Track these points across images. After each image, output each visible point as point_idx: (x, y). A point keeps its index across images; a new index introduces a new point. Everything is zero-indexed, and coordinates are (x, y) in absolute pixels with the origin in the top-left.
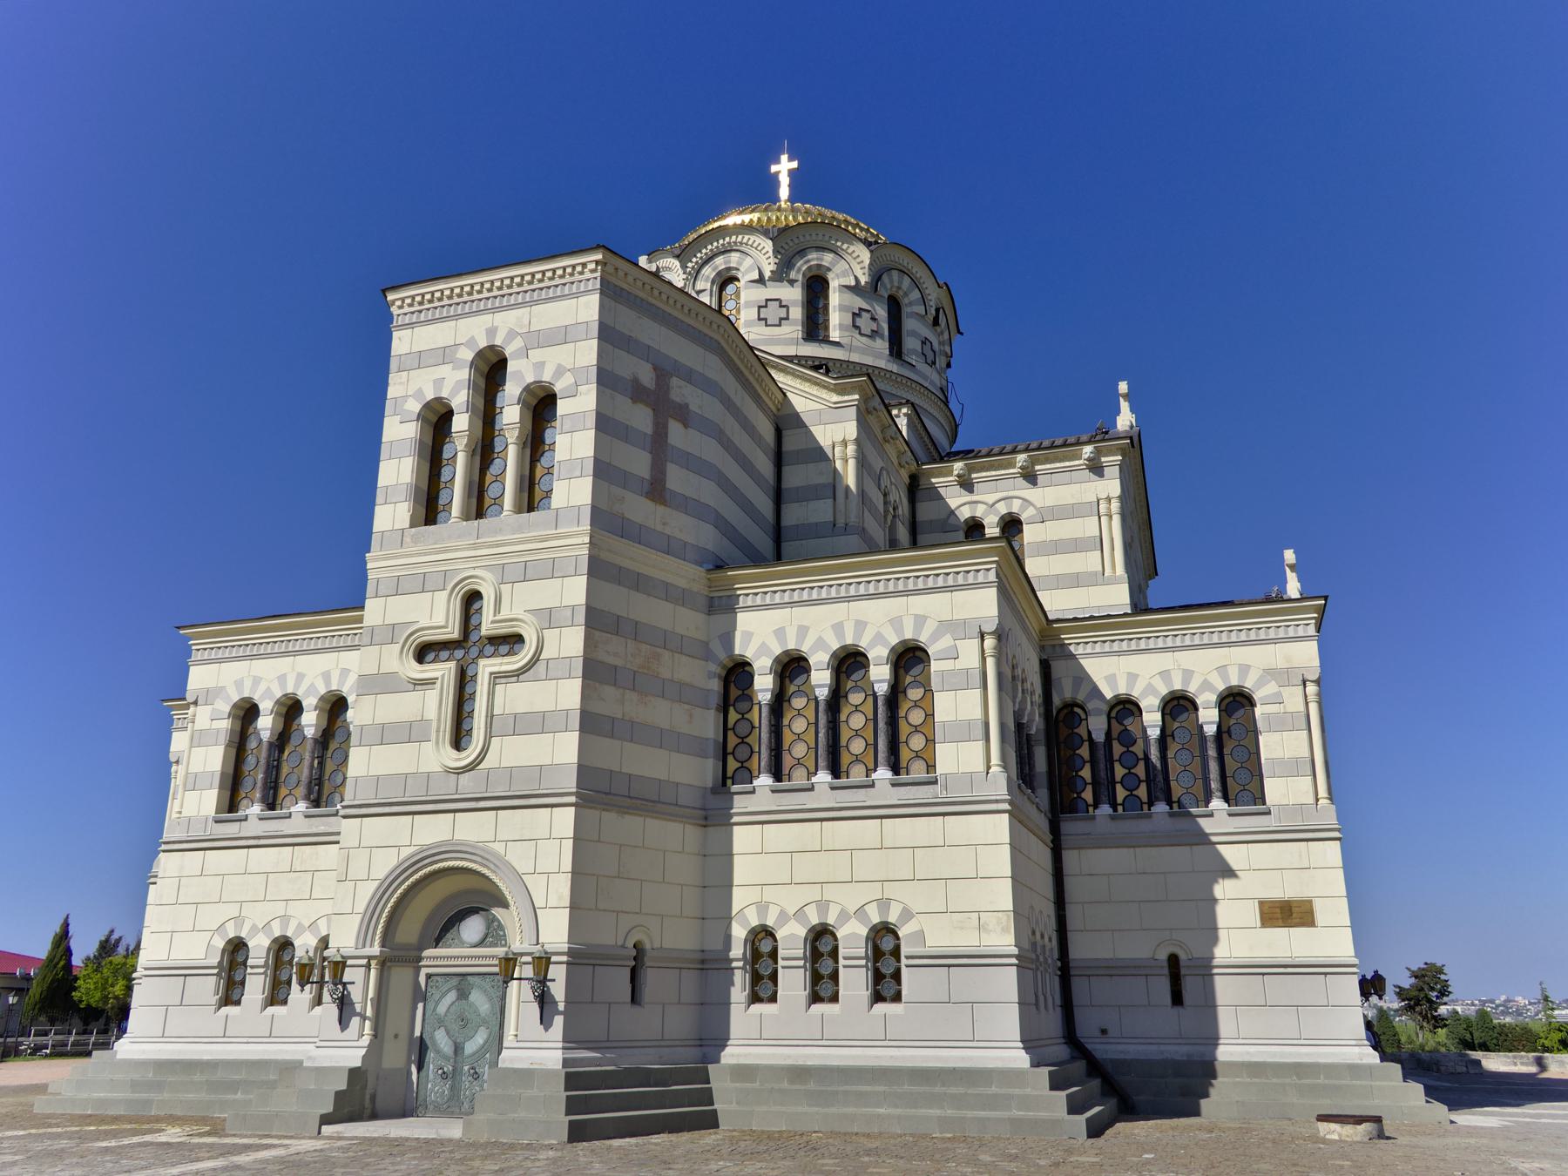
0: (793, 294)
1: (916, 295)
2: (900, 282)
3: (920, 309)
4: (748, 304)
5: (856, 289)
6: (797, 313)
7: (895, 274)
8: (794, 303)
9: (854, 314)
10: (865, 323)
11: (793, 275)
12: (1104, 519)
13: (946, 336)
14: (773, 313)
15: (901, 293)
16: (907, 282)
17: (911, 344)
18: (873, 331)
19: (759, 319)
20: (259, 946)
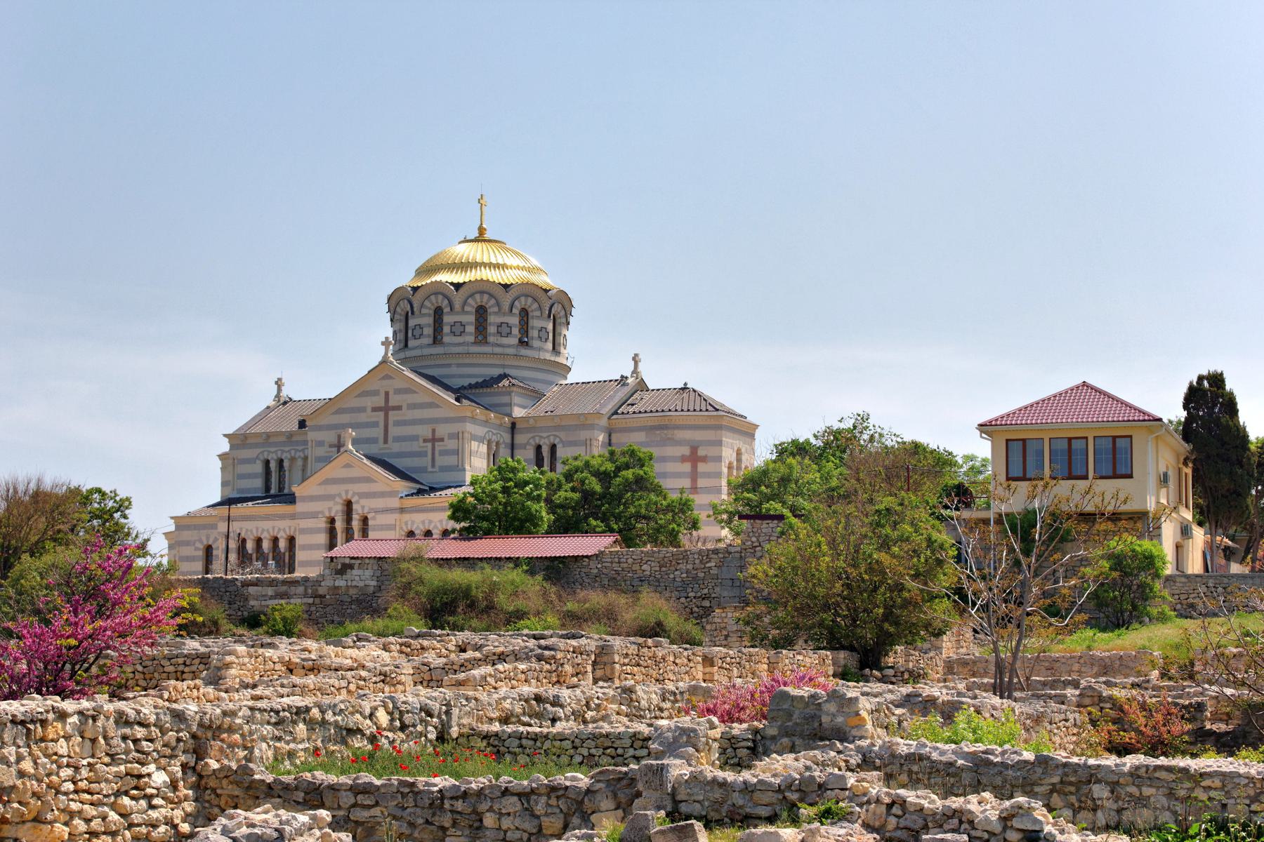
1: (535, 306)
2: (526, 301)
3: (538, 313)
4: (448, 324)
5: (500, 312)
6: (471, 329)
7: (523, 299)
8: (469, 323)
10: (505, 330)
11: (467, 308)
12: (588, 447)
13: (563, 313)
14: (458, 329)
15: (526, 307)
16: (530, 300)
17: (534, 333)
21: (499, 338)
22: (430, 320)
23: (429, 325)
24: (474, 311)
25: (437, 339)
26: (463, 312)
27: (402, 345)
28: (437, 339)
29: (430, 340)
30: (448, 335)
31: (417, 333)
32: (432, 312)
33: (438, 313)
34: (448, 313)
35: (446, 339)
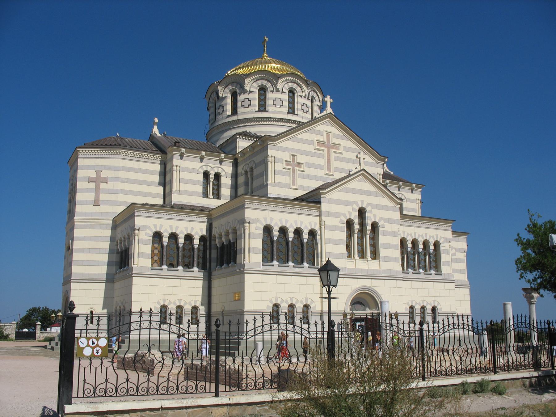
0: (285, 97)
4: (271, 98)
6: (286, 103)
8: (285, 100)
9: (302, 105)
10: (304, 107)
14: (278, 103)
18: (307, 111)
19: (274, 104)
20: (172, 308)
21: (303, 113)
22: (256, 96)
23: (254, 99)
24: (287, 92)
25: (263, 107)
26: (283, 92)
27: (229, 113)
28: (263, 107)
29: (257, 109)
30: (271, 106)
31: (246, 103)
32: (257, 91)
33: (263, 90)
34: (272, 91)
35: (270, 108)
